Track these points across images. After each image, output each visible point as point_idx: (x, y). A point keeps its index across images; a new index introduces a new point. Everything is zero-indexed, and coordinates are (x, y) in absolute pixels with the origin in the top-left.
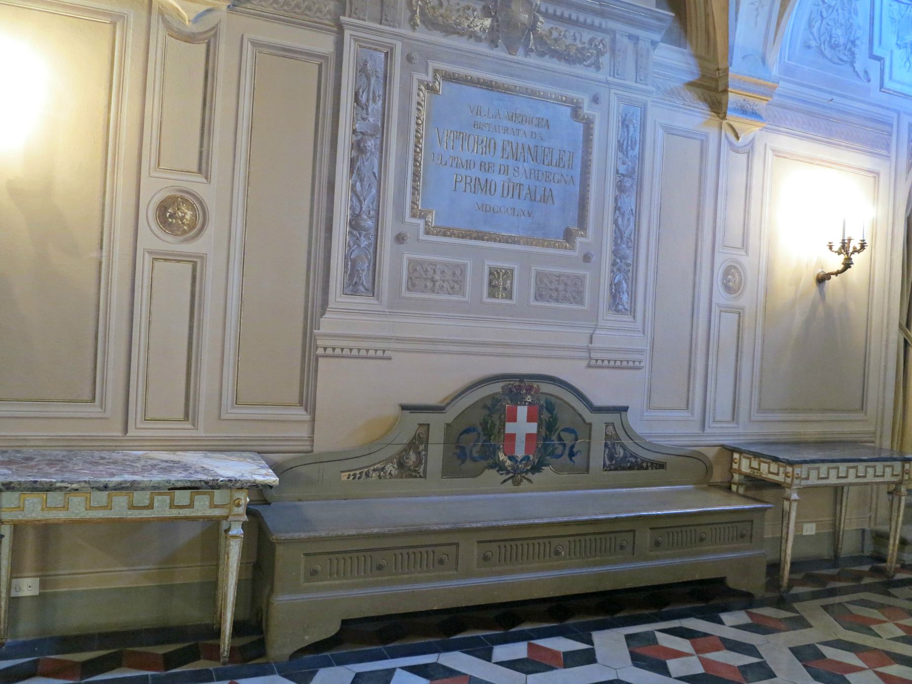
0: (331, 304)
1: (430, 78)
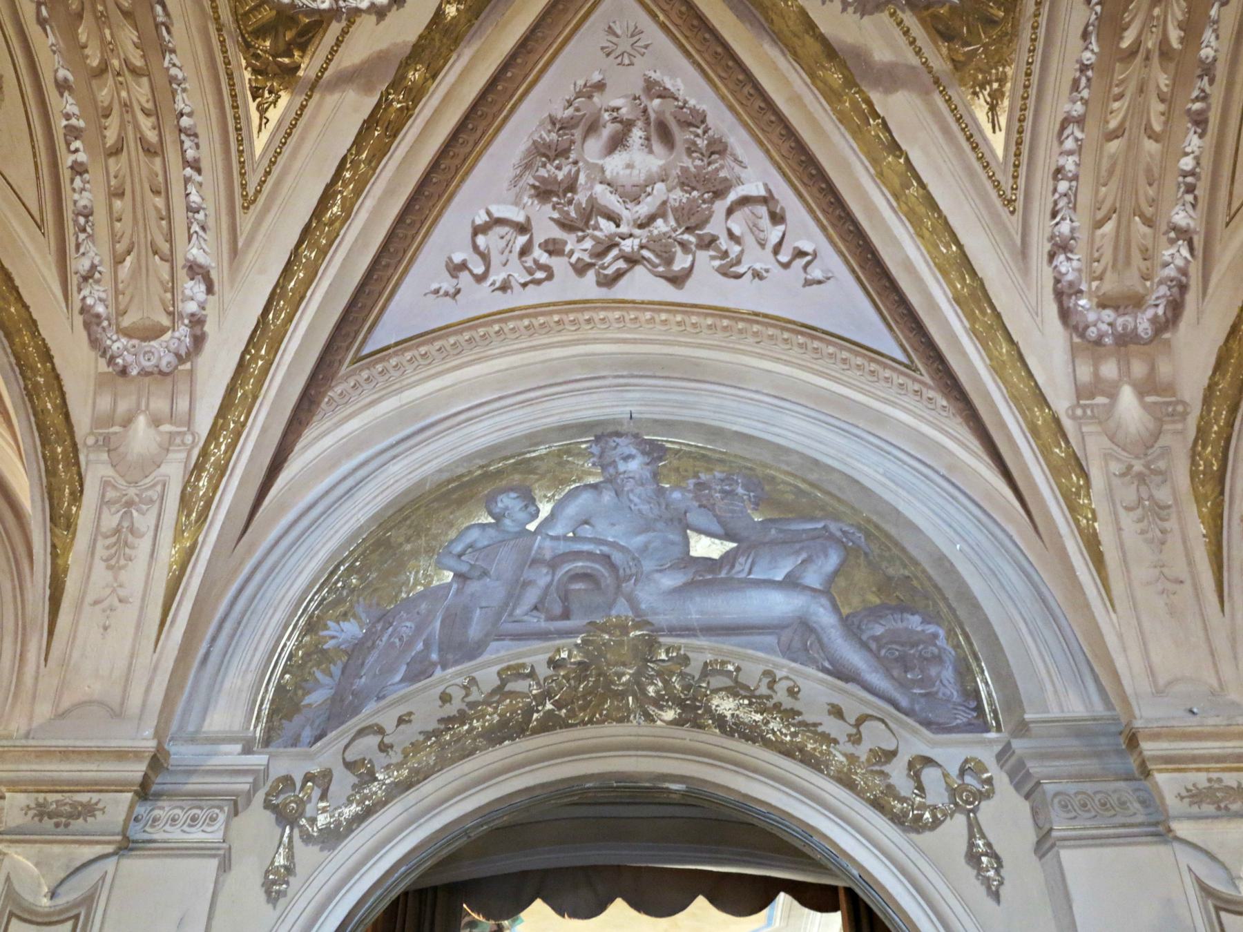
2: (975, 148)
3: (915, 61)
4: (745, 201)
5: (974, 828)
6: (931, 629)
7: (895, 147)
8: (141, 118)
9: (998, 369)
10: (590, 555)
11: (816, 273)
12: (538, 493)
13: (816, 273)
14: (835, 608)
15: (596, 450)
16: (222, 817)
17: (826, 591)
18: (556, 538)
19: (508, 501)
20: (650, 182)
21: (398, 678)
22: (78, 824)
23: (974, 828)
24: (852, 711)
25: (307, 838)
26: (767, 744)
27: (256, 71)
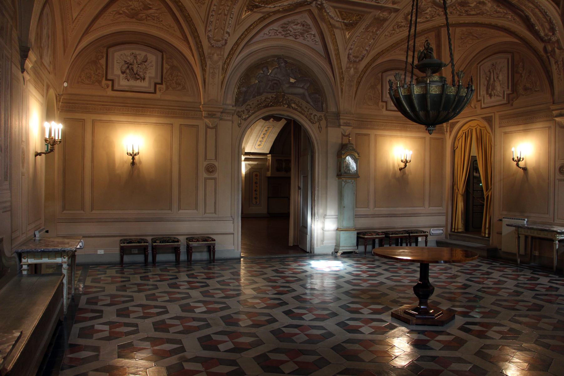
3: (341, 27)
4: (311, 34)
5: (320, 124)
6: (319, 97)
7: (334, 35)
8: (226, 11)
9: (337, 64)
10: (276, 80)
11: (317, 43)
13: (317, 43)
14: (308, 92)
15: (277, 61)
16: (231, 116)
18: (272, 77)
19: (265, 69)
21: (252, 97)
22: (214, 116)
23: (320, 124)
25: (242, 119)
26: (298, 111)
27: (247, 9)
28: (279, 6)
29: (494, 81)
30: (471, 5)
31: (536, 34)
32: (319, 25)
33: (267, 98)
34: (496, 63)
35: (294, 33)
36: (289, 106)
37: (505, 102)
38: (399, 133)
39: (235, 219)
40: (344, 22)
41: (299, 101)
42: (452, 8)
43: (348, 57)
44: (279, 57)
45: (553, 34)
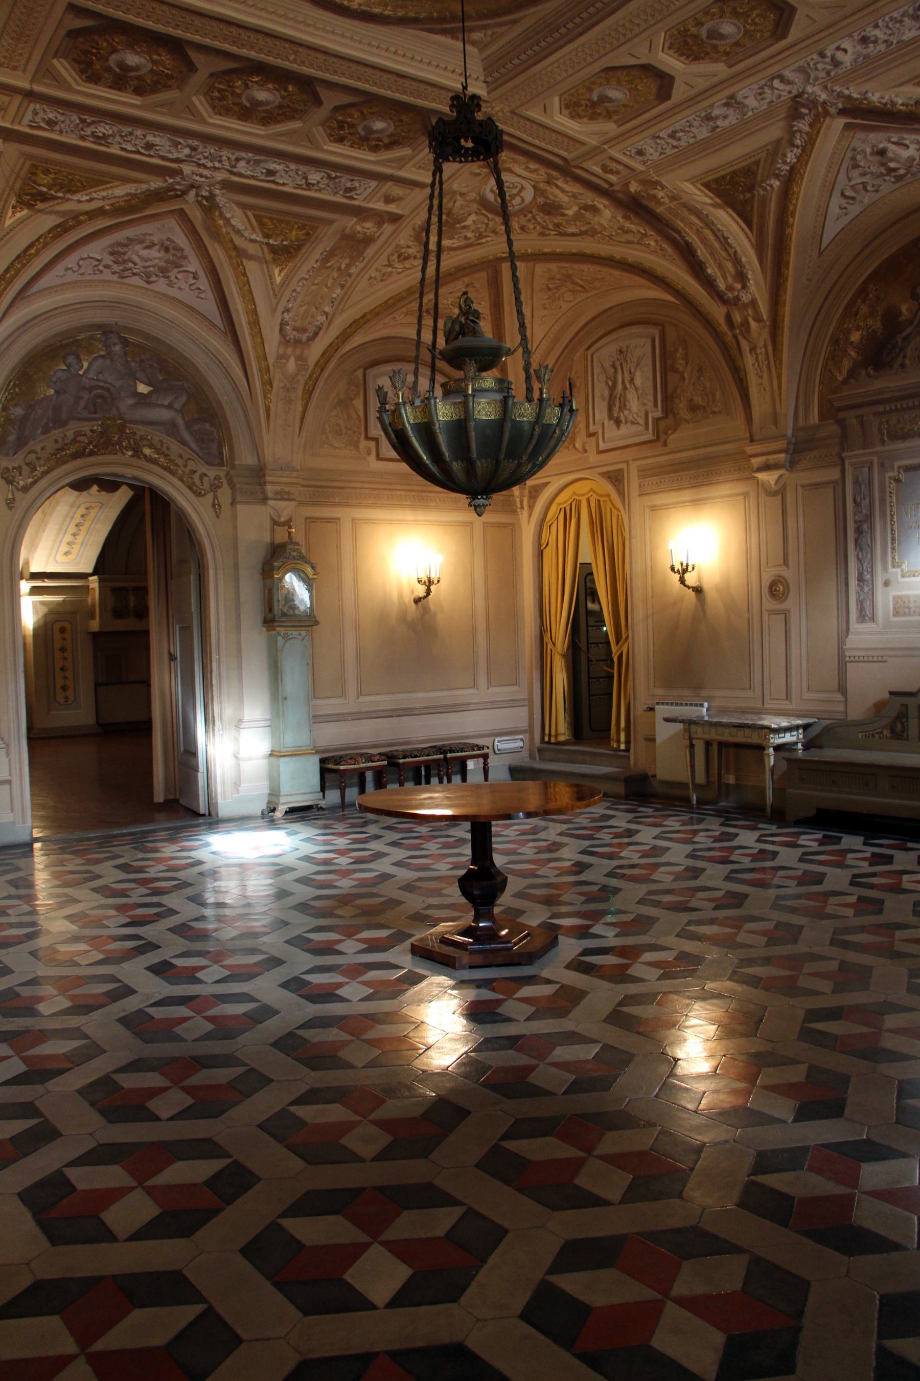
0: (851, 630)
1: (896, 473)
2: (271, 279)
3: (261, 255)
5: (215, 497)
6: (212, 429)
7: (245, 275)
9: (255, 347)
10: (102, 388)
11: (203, 296)
12: (82, 357)
13: (203, 296)
14: (184, 419)
15: (103, 339)
17: (180, 411)
18: (90, 379)
19: (71, 359)
20: (154, 259)
21: (39, 432)
23: (215, 497)
24: (185, 456)
25: (18, 489)
26: (159, 466)
27: (18, 202)
28: (104, 198)
29: (625, 388)
30: (567, 212)
31: (709, 283)
32: (206, 250)
33: (78, 434)
34: (627, 347)
35: (143, 270)
36: (137, 453)
37: (649, 436)
38: (409, 515)
39: (13, 744)
40: (268, 244)
41: (161, 441)
42: (525, 216)
43: (281, 330)
44: (106, 330)
45: (744, 287)
